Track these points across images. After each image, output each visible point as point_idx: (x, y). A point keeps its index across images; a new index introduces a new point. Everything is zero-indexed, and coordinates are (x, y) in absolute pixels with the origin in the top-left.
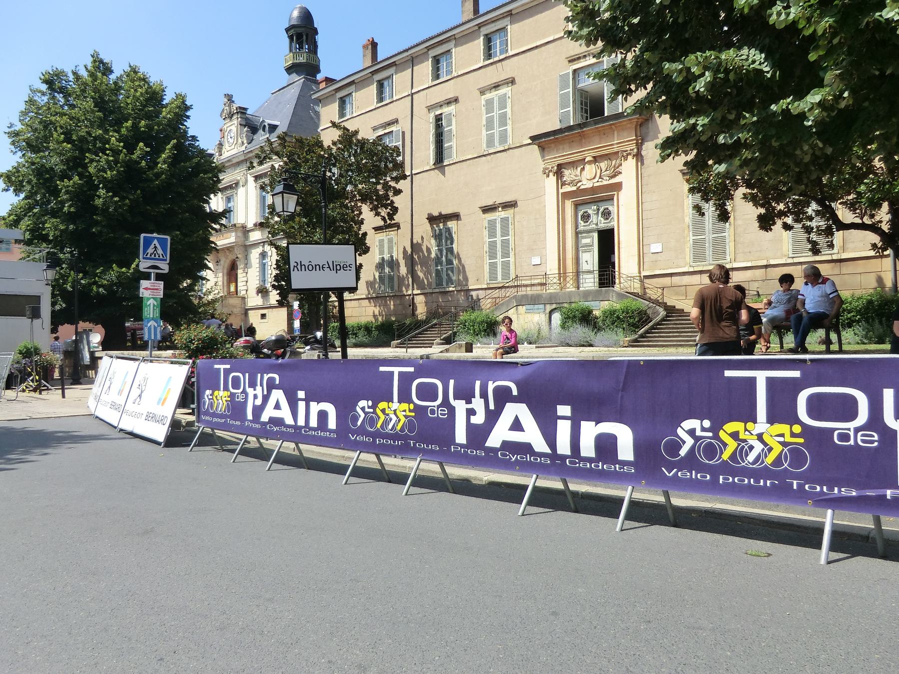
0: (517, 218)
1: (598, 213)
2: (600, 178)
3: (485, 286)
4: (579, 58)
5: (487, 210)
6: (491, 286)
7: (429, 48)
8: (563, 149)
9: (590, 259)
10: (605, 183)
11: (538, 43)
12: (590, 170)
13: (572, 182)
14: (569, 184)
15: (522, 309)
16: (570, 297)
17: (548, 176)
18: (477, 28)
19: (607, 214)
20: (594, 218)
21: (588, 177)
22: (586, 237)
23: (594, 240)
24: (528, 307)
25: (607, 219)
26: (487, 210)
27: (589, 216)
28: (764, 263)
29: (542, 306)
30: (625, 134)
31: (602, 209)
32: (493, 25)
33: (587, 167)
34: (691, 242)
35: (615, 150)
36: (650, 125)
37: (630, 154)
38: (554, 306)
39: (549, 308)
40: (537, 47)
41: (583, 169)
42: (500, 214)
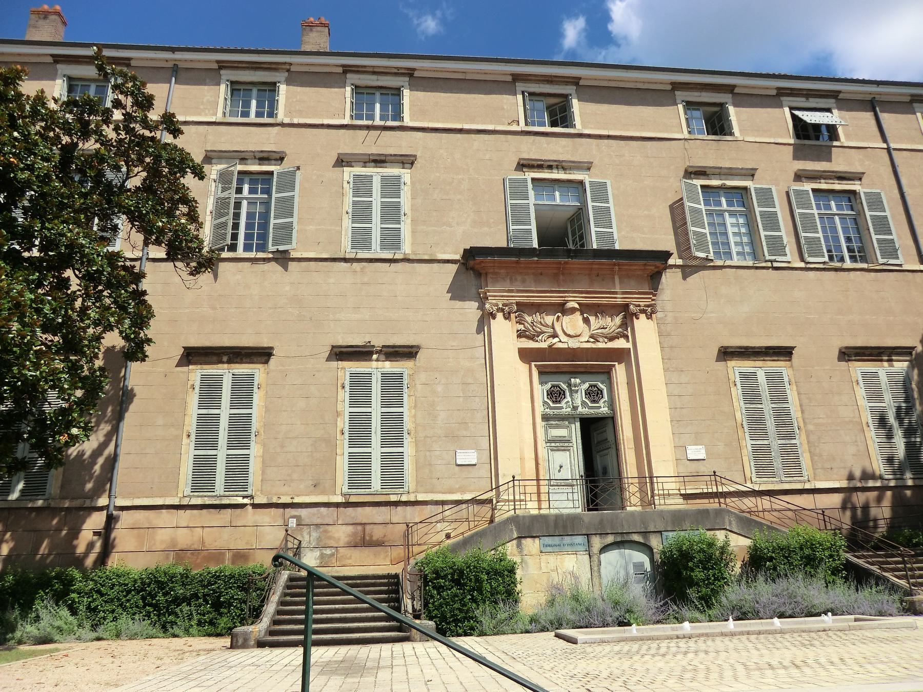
0: (422, 377)
2: (592, 336)
3: (340, 499)
5: (341, 354)
6: (353, 499)
10: (600, 345)
11: (466, 126)
15: (532, 545)
16: (644, 523)
18: (340, 70)
22: (557, 427)
23: (574, 432)
24: (548, 540)
25: (594, 401)
26: (341, 354)
29: (580, 539)
30: (633, 283)
32: (374, 77)
34: (750, 448)
35: (619, 301)
38: (610, 539)
39: (597, 543)
40: (460, 131)
42: (378, 368)
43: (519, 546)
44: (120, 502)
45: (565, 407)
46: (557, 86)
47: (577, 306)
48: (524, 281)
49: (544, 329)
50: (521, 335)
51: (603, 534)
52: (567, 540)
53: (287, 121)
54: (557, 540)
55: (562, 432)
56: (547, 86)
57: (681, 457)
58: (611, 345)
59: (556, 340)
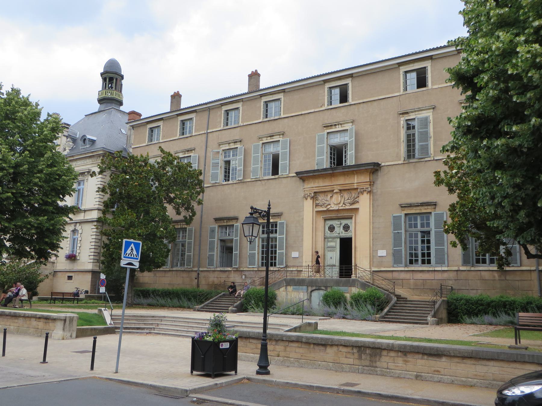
1: (340, 227)
2: (344, 204)
4: (331, 126)
7: (222, 105)
8: (318, 182)
9: (333, 257)
10: (347, 207)
11: (303, 113)
12: (337, 198)
13: (324, 204)
14: (321, 206)
15: (290, 288)
17: (306, 199)
19: (346, 228)
20: (337, 230)
21: (335, 202)
22: (331, 241)
24: (295, 287)
25: (347, 231)
27: (334, 228)
28: (456, 268)
29: (305, 287)
31: (343, 225)
32: (271, 96)
33: (335, 196)
35: (355, 187)
36: (379, 174)
37: (366, 191)
38: (314, 288)
39: (310, 289)
41: (332, 197)
43: (286, 288)
44: (201, 269)
45: (334, 234)
46: (343, 80)
47: (338, 191)
48: (318, 182)
49: (326, 202)
50: (317, 205)
51: (312, 286)
52: (301, 287)
53: (242, 125)
54: (297, 287)
55: (332, 244)
56: (339, 81)
57: (373, 257)
58: (351, 207)
59: (329, 206)
